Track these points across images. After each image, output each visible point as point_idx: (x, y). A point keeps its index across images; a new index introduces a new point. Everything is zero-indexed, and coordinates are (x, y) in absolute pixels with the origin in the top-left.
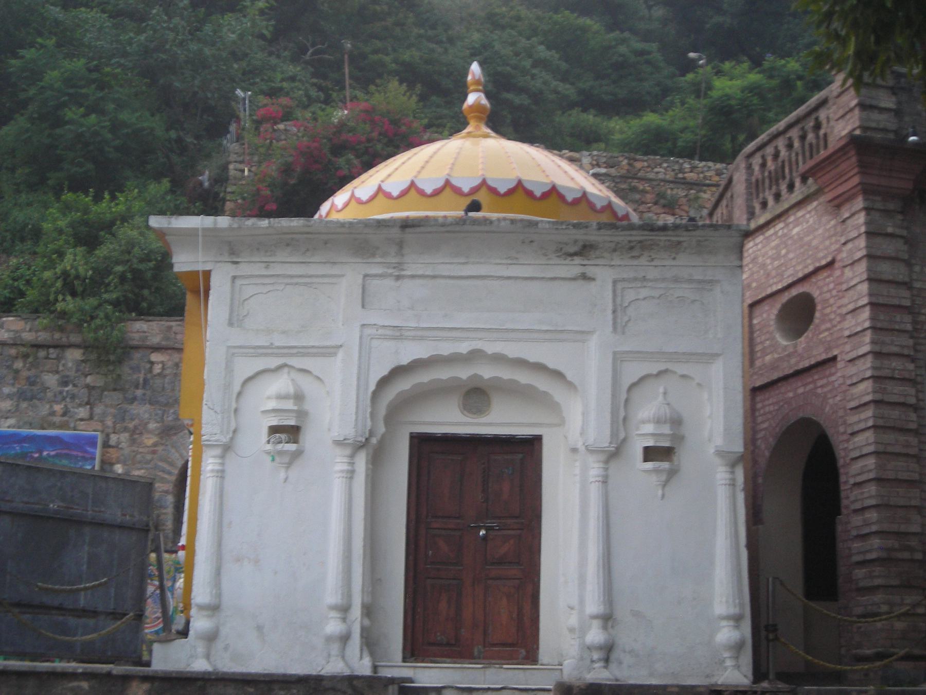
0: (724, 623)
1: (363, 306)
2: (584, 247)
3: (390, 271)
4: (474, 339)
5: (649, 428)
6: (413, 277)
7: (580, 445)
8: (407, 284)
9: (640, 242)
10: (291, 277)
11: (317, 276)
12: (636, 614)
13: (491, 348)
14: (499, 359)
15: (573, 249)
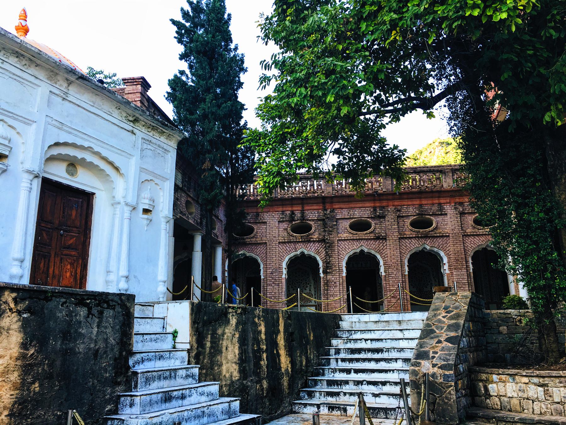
0: (161, 283)
1: (48, 106)
2: (135, 120)
3: (62, 95)
4: (90, 142)
5: (147, 201)
6: (70, 101)
7: (122, 201)
8: (66, 103)
9: (153, 126)
10: (14, 74)
11: (27, 80)
12: (135, 277)
13: (96, 149)
14: (97, 154)
15: (131, 119)
